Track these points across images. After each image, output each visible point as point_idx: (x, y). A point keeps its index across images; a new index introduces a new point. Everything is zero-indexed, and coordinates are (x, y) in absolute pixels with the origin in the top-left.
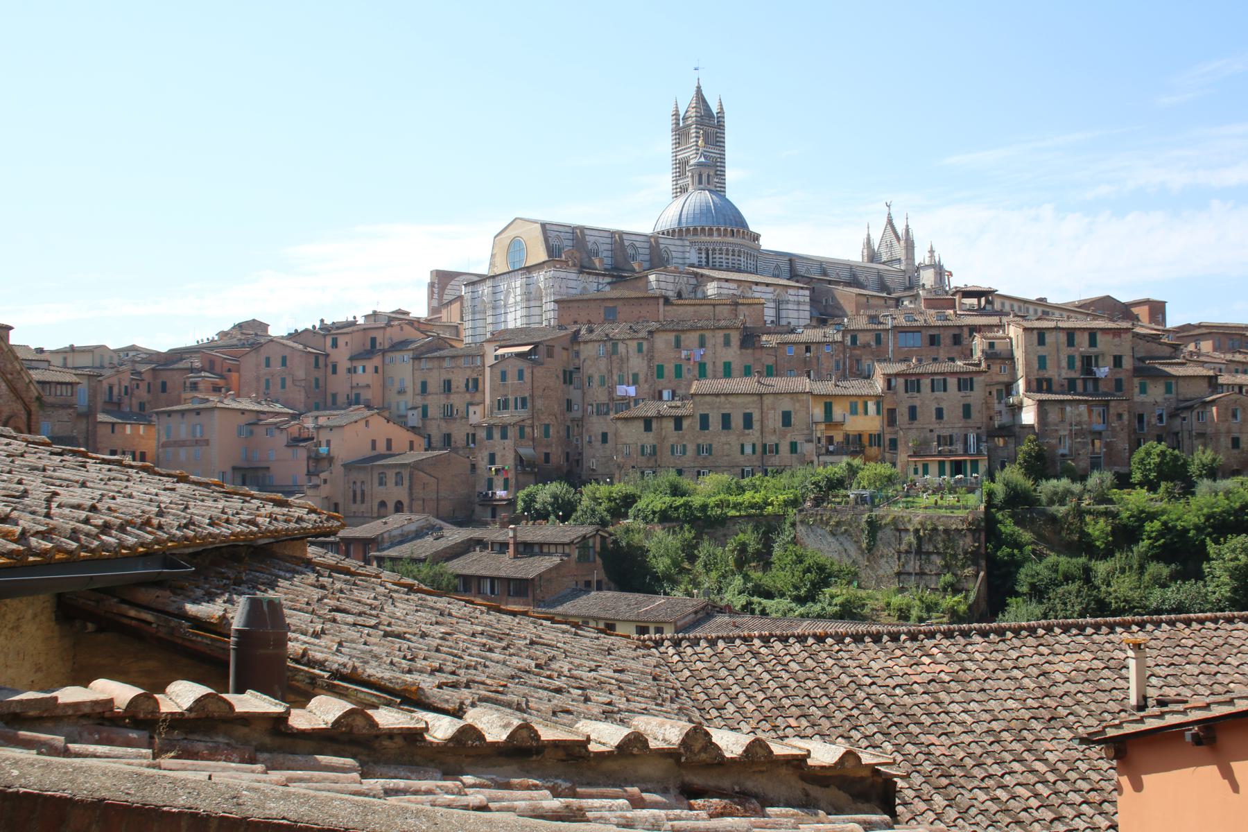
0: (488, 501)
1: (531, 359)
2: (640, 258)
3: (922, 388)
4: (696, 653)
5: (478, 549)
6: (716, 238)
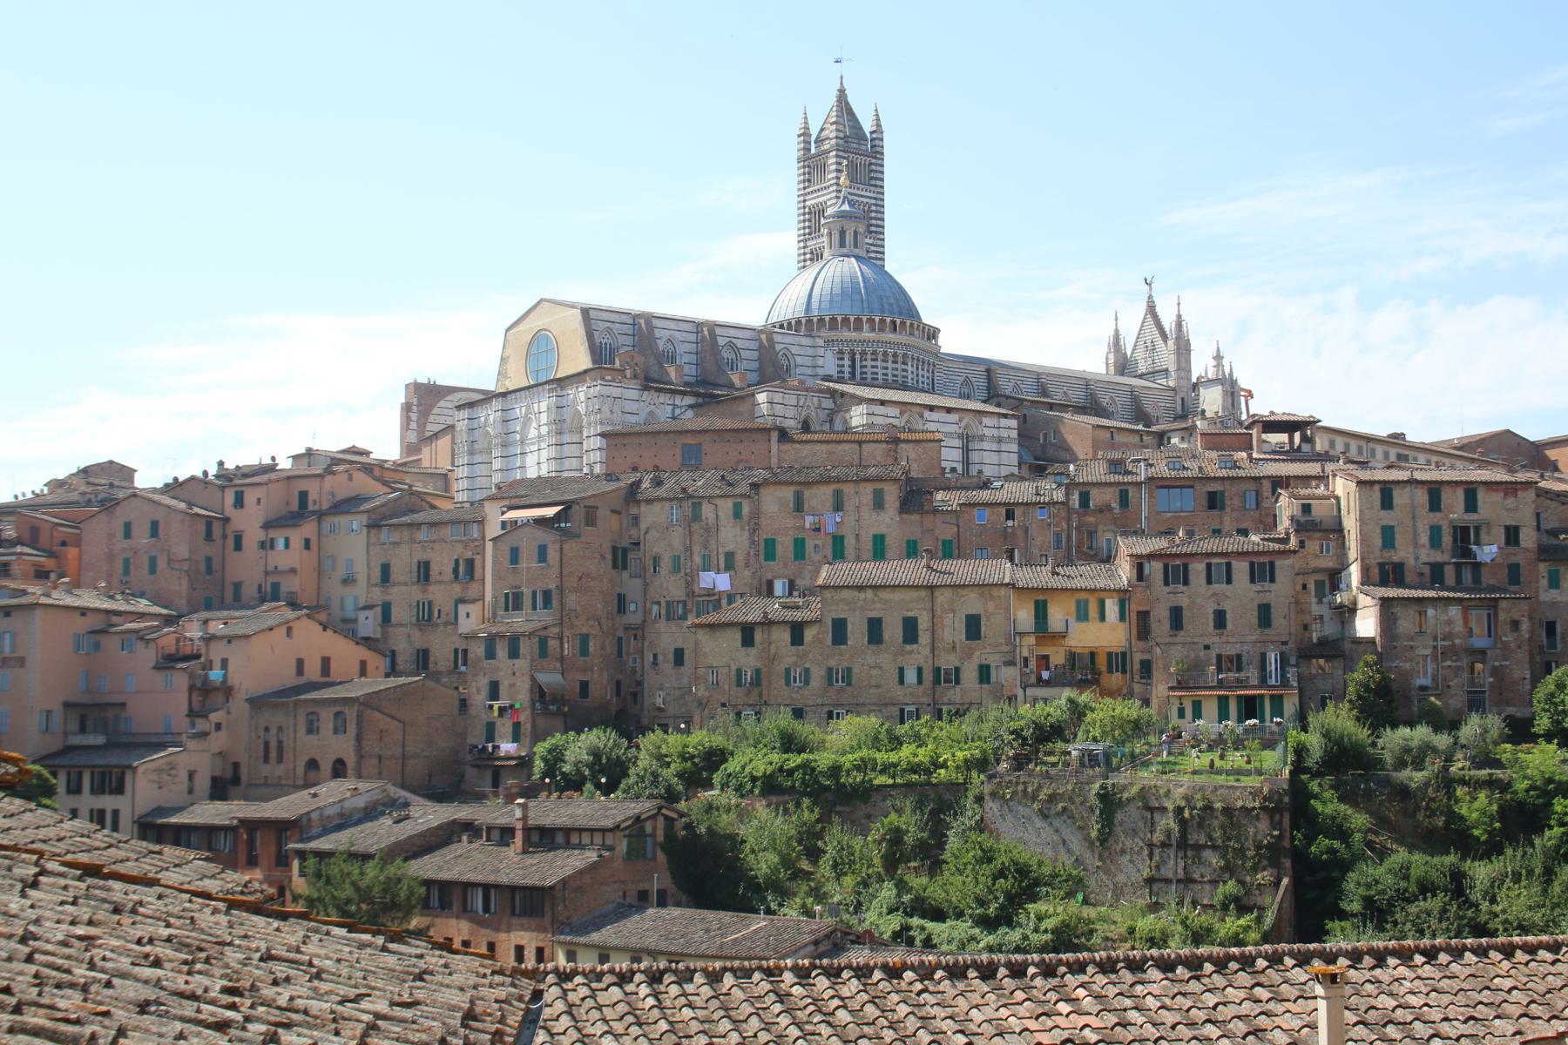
0: (486, 760)
1: (557, 529)
2: (743, 365)
3: (1192, 578)
4: (685, 995)
5: (465, 838)
6: (866, 334)
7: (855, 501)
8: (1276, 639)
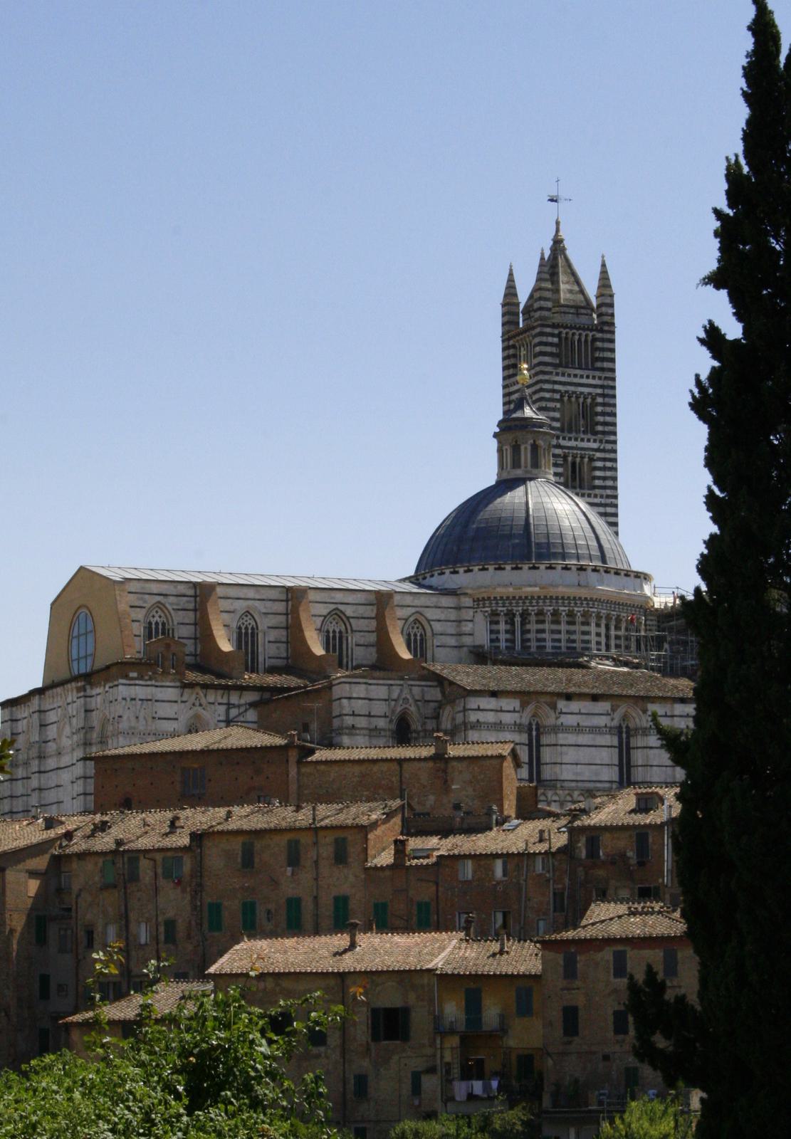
7: (312, 854)
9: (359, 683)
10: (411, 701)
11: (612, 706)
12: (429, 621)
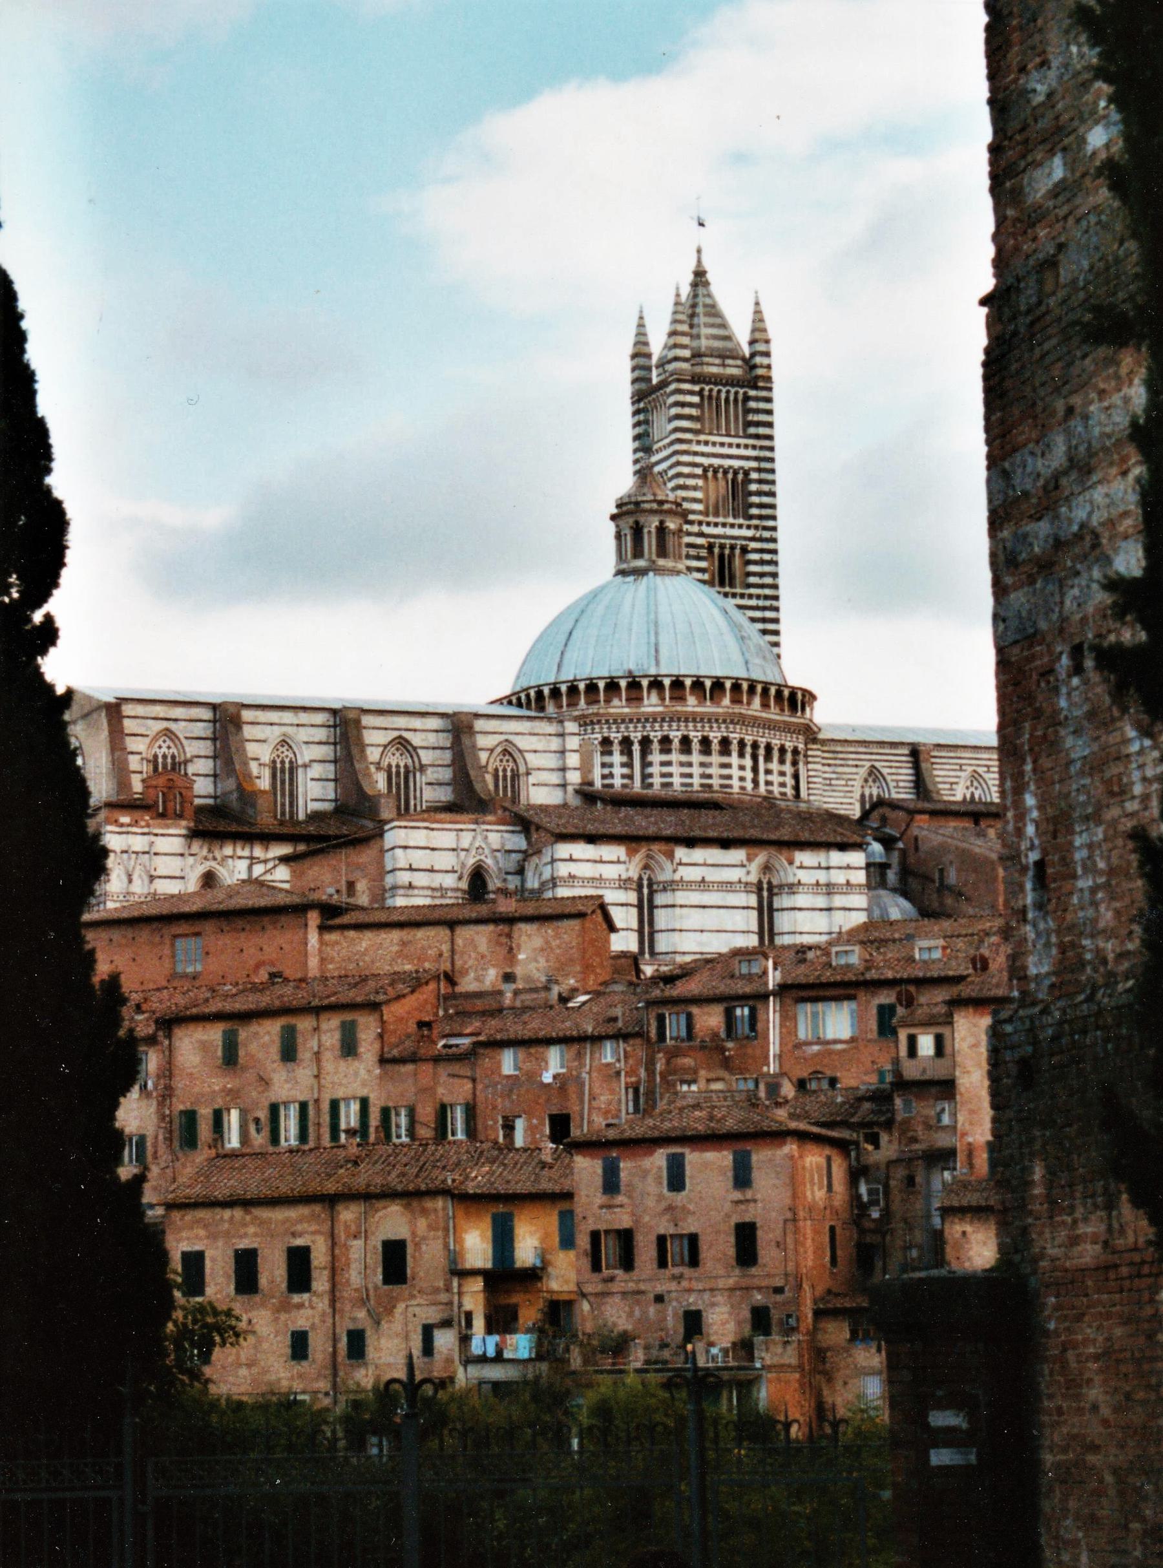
8: (765, 1283)
9: (418, 828)
10: (487, 851)
11: (748, 855)
12: (520, 751)
